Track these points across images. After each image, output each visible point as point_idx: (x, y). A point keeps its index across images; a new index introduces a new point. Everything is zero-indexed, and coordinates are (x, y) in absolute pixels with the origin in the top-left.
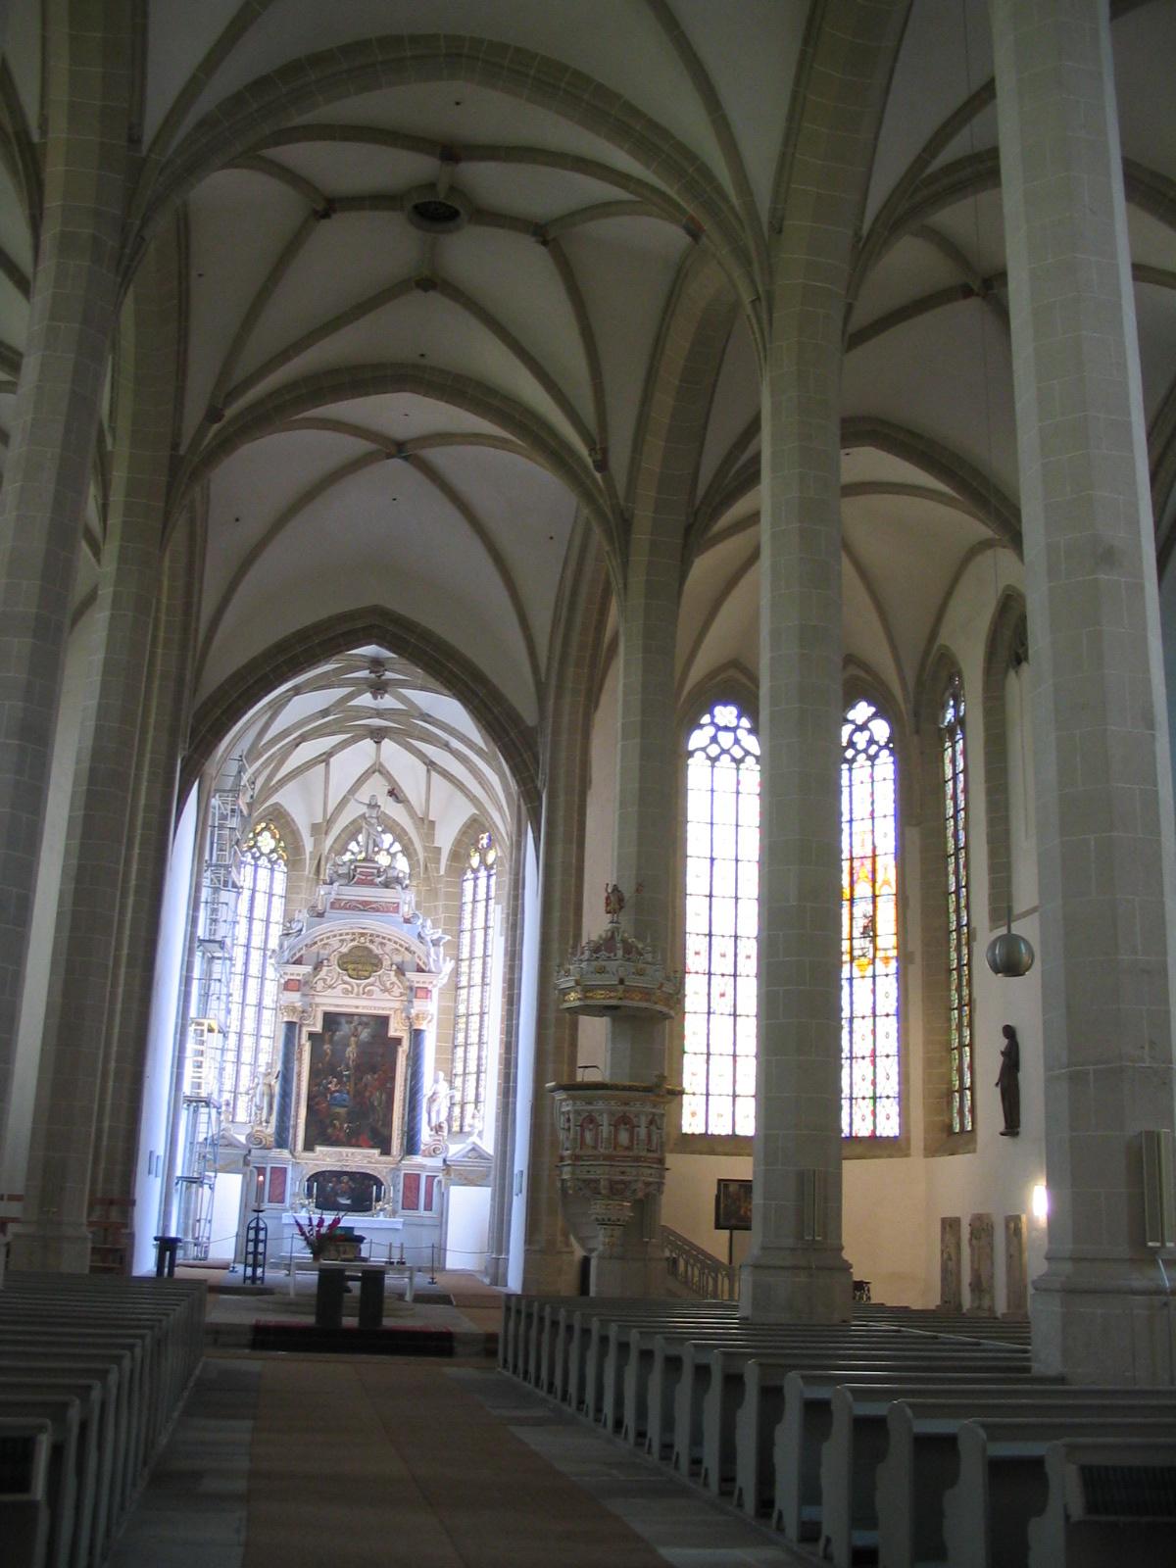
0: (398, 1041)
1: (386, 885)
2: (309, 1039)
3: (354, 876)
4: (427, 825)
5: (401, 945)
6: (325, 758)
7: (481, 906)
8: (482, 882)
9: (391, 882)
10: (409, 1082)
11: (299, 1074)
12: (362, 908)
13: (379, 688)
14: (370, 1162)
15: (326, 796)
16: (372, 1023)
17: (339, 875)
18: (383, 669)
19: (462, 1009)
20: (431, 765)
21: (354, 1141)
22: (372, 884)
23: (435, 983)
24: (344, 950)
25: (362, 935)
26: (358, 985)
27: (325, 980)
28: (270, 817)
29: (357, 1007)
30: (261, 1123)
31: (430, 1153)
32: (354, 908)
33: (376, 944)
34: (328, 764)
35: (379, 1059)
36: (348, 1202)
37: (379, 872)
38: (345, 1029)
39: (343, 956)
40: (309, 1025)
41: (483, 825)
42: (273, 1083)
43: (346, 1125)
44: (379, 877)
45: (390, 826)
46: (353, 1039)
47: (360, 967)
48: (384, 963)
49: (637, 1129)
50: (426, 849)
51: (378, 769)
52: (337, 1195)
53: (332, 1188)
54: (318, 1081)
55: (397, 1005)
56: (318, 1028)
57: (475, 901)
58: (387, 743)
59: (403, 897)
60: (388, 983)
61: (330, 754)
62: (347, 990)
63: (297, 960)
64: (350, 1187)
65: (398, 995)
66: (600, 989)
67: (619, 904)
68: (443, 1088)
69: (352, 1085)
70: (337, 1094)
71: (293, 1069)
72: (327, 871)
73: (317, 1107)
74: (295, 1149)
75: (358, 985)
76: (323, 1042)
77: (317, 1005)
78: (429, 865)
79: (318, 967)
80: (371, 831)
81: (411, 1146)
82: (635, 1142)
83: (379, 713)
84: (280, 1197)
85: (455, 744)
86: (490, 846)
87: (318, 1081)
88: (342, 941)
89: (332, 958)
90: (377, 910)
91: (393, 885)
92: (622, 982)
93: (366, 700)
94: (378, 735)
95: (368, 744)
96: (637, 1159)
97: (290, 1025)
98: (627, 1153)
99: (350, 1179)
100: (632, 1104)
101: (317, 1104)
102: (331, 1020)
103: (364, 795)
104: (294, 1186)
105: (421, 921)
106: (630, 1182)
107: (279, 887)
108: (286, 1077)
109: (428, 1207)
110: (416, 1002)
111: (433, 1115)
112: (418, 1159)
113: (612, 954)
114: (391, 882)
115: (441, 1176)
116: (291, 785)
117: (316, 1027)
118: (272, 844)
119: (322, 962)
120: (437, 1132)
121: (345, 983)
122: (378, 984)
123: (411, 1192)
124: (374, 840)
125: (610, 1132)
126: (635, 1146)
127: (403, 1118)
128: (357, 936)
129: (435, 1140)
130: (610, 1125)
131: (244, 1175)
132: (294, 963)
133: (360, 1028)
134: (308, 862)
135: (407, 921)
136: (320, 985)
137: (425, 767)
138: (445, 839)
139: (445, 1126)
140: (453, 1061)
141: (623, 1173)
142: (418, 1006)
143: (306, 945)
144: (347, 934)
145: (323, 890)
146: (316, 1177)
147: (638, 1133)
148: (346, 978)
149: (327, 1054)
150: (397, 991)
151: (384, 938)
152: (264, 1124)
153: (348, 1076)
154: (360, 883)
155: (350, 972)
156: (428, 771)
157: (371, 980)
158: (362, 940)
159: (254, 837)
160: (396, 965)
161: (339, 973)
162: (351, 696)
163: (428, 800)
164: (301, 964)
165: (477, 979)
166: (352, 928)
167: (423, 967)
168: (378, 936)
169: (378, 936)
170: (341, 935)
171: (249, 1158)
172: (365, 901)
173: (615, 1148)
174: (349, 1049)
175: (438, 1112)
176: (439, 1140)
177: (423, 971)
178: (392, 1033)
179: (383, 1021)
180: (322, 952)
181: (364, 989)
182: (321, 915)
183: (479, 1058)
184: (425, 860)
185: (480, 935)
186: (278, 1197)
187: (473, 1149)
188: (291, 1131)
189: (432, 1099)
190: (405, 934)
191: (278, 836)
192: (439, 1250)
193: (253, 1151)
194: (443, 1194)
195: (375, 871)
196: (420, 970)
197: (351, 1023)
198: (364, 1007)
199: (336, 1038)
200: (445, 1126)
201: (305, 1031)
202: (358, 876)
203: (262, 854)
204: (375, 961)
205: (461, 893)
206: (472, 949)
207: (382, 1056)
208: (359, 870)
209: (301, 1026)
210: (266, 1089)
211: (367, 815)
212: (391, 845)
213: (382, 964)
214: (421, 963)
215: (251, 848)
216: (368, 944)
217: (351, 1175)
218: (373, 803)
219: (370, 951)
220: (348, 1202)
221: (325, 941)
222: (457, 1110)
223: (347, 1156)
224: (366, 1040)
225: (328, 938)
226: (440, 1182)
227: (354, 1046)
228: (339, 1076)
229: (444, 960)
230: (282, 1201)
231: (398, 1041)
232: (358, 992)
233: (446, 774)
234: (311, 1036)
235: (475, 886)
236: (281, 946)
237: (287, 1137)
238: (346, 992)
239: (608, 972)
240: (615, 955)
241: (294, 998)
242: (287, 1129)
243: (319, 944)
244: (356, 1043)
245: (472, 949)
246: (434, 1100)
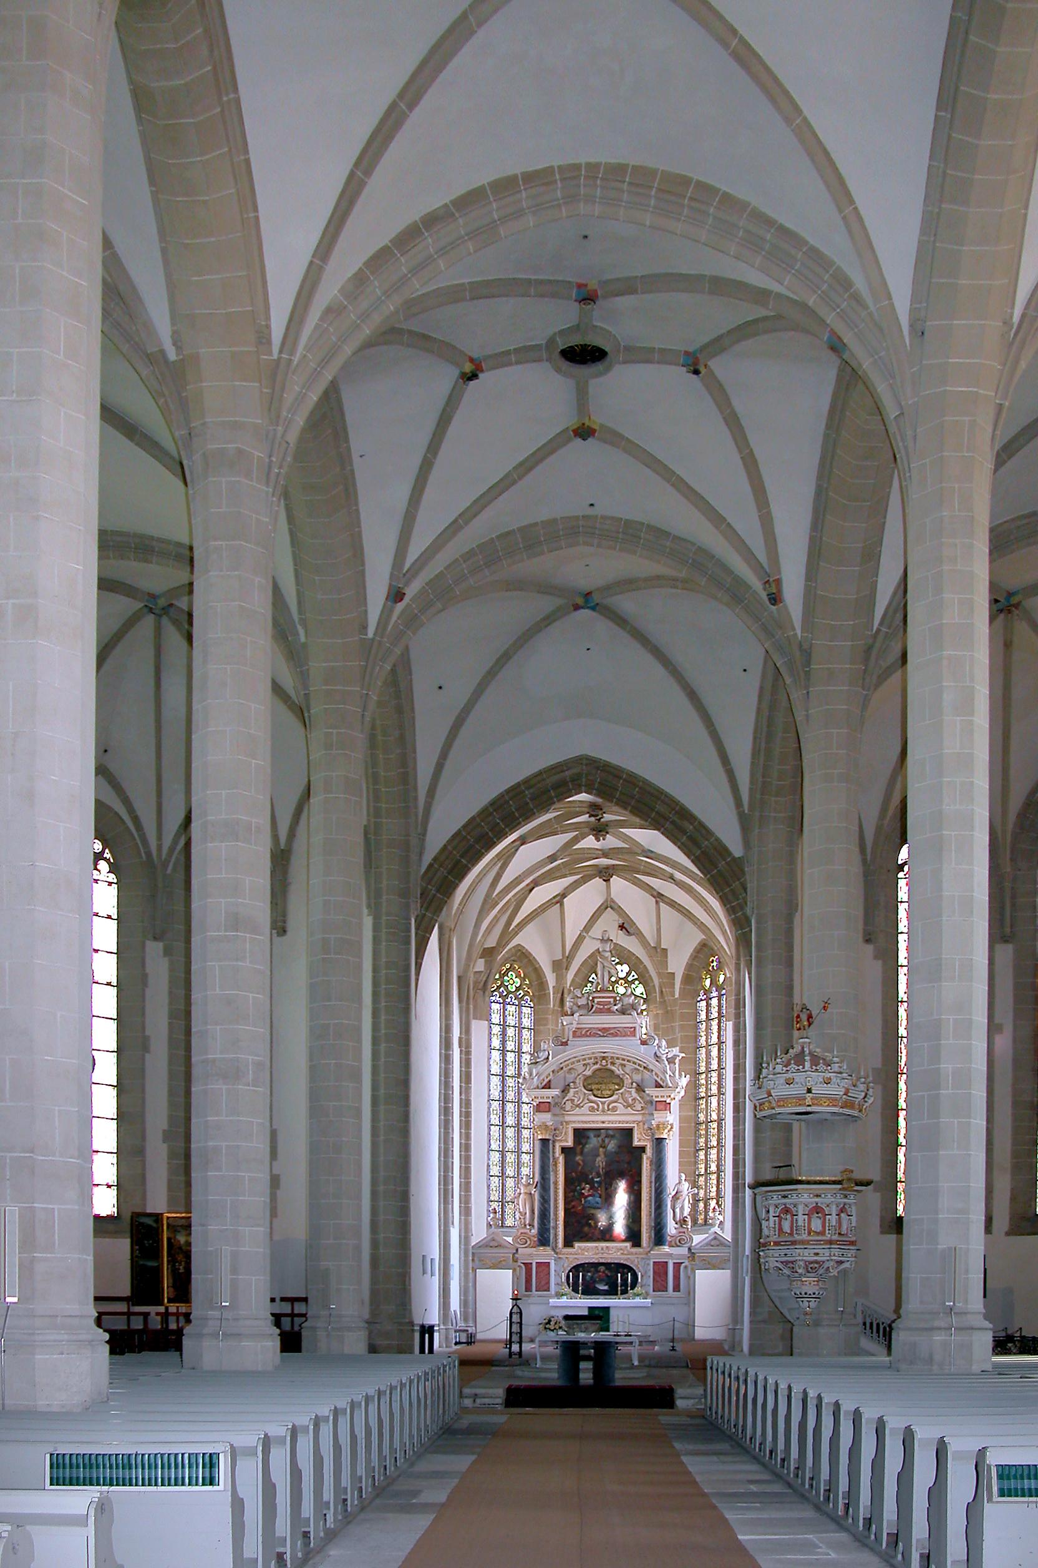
0: (643, 1149)
1: (623, 1012)
2: (562, 1153)
3: (593, 1006)
4: (660, 953)
5: (639, 1065)
6: (559, 900)
7: (715, 1023)
8: (714, 1002)
9: (627, 1010)
10: (653, 1184)
11: (556, 1183)
12: (602, 1034)
13: (599, 831)
14: (622, 1254)
15: (563, 934)
16: (617, 1135)
17: (579, 1007)
18: (601, 812)
19: (702, 1117)
20: (659, 897)
22: (609, 1011)
23: (672, 1096)
24: (588, 1073)
25: (604, 1058)
26: (603, 1103)
27: (573, 1101)
28: (512, 958)
29: (603, 1122)
30: (525, 1225)
31: (676, 1244)
32: (595, 1035)
34: (562, 905)
35: (626, 1166)
36: (606, 1288)
37: (615, 1000)
38: (594, 1142)
39: (587, 1078)
40: (561, 1141)
41: (712, 949)
42: (533, 1192)
44: (615, 1005)
45: (624, 956)
46: (601, 1149)
47: (603, 1087)
48: (625, 1082)
50: (659, 974)
51: (609, 905)
52: (595, 1282)
53: (592, 1277)
54: (573, 1187)
55: (639, 1118)
56: (570, 1143)
57: (708, 1019)
58: (614, 879)
59: (639, 1022)
60: (630, 1099)
61: (563, 895)
62: (593, 1107)
63: (546, 1085)
64: (607, 1276)
65: (640, 1109)
68: (686, 1186)
69: (603, 1189)
70: (590, 1198)
71: (549, 1180)
72: (568, 1004)
73: (572, 1210)
74: (556, 1246)
75: (603, 1103)
76: (575, 1154)
77: (567, 1123)
78: (664, 990)
79: (565, 1090)
80: (605, 964)
81: (659, 1238)
83: (605, 854)
84: (545, 1288)
85: (678, 876)
86: (720, 968)
87: (573, 1187)
88: (584, 1065)
89: (577, 1081)
90: (616, 1035)
91: (628, 1012)
93: (590, 842)
94: (606, 874)
95: (598, 882)
97: (544, 1142)
99: (607, 1269)
101: (573, 1207)
102: (580, 1134)
103: (596, 931)
104: (557, 1275)
105: (657, 1042)
107: (526, 1022)
108: (544, 1185)
109: (677, 1288)
110: (656, 1114)
111: (678, 1210)
112: (666, 1249)
114: (627, 1010)
115: (687, 1263)
116: (530, 928)
117: (567, 1142)
118: (518, 982)
119: (568, 1085)
120: (681, 1226)
122: (621, 1101)
123: (660, 1276)
124: (609, 972)
127: (650, 1215)
128: (599, 1060)
129: (680, 1232)
131: (514, 1270)
132: (543, 1088)
133: (607, 1140)
134: (552, 996)
135: (644, 1043)
136: (568, 1105)
137: (654, 900)
138: (678, 964)
139: (689, 1220)
140: (696, 1163)
142: (658, 1117)
143: (553, 1071)
144: (590, 1058)
145: (566, 1020)
146: (576, 1269)
148: (593, 1098)
149: (579, 1164)
150: (638, 1107)
151: (624, 1060)
152: (528, 1227)
153: (599, 1183)
154: (600, 1012)
155: (595, 1092)
156: (657, 902)
159: (500, 977)
160: (636, 1083)
161: (585, 1094)
162: (576, 840)
163: (659, 930)
164: (550, 1088)
165: (714, 1089)
166: (593, 1053)
167: (662, 1083)
168: (618, 1058)
169: (618, 1058)
170: (585, 1060)
171: (516, 1255)
172: (604, 1028)
174: (598, 1159)
175: (682, 1209)
176: (684, 1232)
177: (661, 1087)
178: (636, 1143)
179: (629, 1132)
180: (567, 1075)
182: (565, 1044)
183: (719, 1159)
184: (660, 987)
185: (714, 1052)
186: (544, 1286)
187: (715, 1238)
188: (552, 1231)
189: (676, 1197)
190: (644, 1053)
191: (522, 975)
192: (690, 1324)
193: (519, 1250)
194: (689, 1277)
195: (612, 1000)
196: (658, 1086)
197: (599, 1136)
198: (609, 1122)
199: (586, 1150)
200: (689, 1220)
201: (558, 1145)
203: (510, 992)
204: (617, 1081)
205: (696, 1013)
206: (708, 1063)
207: (629, 1163)
208: (596, 1000)
209: (554, 1142)
210: (526, 1197)
211: (600, 950)
212: (628, 974)
213: (623, 1082)
214: (659, 1080)
215: (499, 987)
216: (609, 1066)
217: (607, 1265)
218: (605, 938)
219: (612, 1072)
220: (606, 1288)
221: (570, 1066)
222: (701, 1205)
223: (602, 1249)
224: (613, 1150)
225: (573, 1063)
226: (686, 1267)
227: (603, 1156)
228: (591, 1183)
229: (680, 1075)
230: (548, 1290)
231: (643, 1149)
232: (603, 1108)
233: (672, 904)
234: (564, 1150)
235: (708, 1005)
236: (531, 1074)
237: (549, 1237)
238: (592, 1109)
241: (546, 1118)
242: (548, 1230)
243: (564, 1069)
244: (605, 1153)
245: (708, 1063)
246: (678, 1199)
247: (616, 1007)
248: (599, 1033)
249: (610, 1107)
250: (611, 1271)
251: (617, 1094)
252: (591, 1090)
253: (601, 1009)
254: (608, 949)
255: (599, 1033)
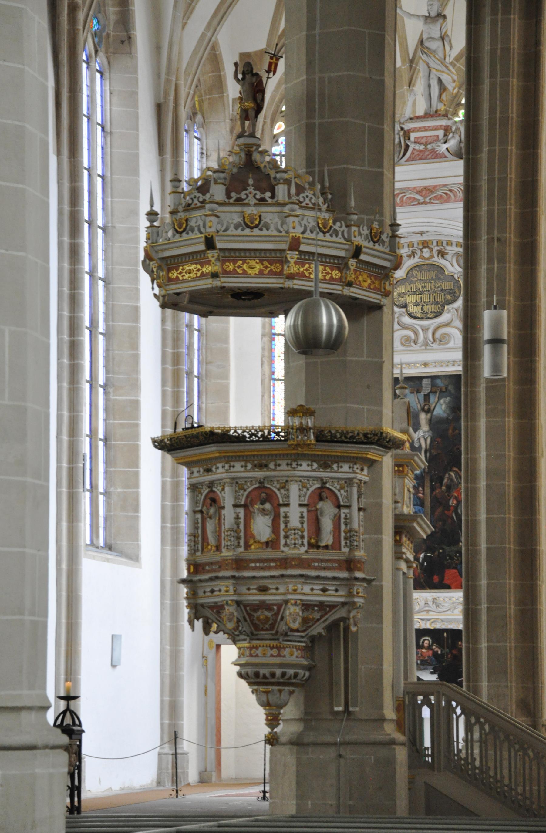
21: (436, 579)
25: (425, 244)
26: (425, 329)
29: (426, 365)
33: (448, 257)
43: (422, 555)
44: (445, 143)
47: (425, 298)
49: (283, 510)
62: (408, 339)
66: (186, 263)
67: (255, 99)
69: (428, 491)
75: (425, 329)
80: (432, 65)
82: (282, 534)
92: (210, 243)
96: (285, 563)
98: (269, 553)
100: (272, 465)
106: (279, 606)
113: (268, 194)
121: (405, 327)
124: (440, 81)
125: (237, 518)
126: (283, 541)
130: (235, 506)
133: (433, 399)
141: (263, 590)
147: (286, 517)
148: (407, 320)
155: (412, 309)
157: (445, 317)
158: (426, 253)
169: (449, 243)
172: (426, 188)
173: (247, 546)
181: (433, 334)
195: (441, 133)
198: (436, 363)
202: (412, 146)
208: (413, 136)
211: (425, 37)
216: (438, 260)
218: (433, 14)
219: (441, 269)
223: (426, 603)
224: (445, 415)
239: (192, 230)
240: (273, 197)
247: (445, 146)
248: (417, 197)
249: (438, 335)
250: (440, 646)
251: (449, 312)
252: (405, 306)
253: (421, 151)
254: (437, 35)
255: (417, 197)
